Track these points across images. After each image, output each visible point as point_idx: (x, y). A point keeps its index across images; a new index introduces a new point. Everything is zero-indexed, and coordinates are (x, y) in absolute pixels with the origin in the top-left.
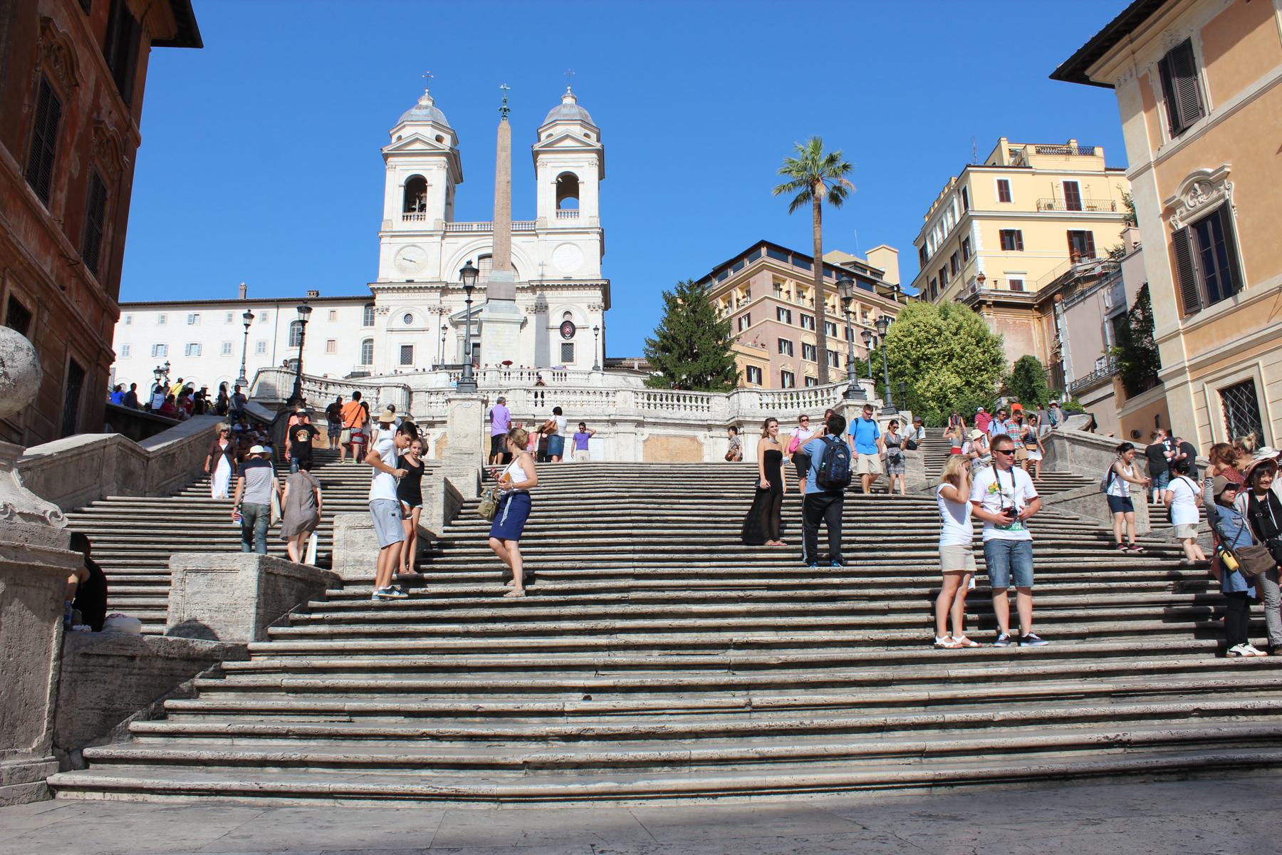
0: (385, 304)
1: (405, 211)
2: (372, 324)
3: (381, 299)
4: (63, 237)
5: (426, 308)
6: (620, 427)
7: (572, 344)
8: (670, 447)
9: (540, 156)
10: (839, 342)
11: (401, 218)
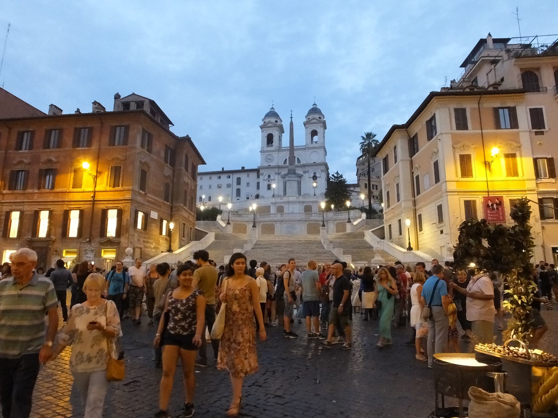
0: (263, 172)
1: (267, 144)
2: (259, 178)
3: (261, 172)
9: (306, 125)
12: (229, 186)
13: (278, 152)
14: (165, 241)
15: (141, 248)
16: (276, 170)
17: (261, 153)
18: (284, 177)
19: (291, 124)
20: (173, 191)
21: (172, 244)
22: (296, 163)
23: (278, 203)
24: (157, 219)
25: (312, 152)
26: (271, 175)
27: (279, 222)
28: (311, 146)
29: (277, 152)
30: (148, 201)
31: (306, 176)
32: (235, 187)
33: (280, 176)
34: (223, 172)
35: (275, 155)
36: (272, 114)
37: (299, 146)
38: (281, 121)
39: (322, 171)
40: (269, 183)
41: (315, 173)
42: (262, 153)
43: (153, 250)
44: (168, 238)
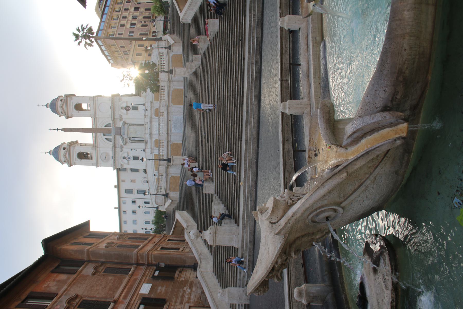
0: (120, 165)
1: (89, 159)
2: (126, 169)
4: (145, 243)
6: (170, 111)
9: (69, 116)
10: (129, 14)
12: (134, 202)
13: (97, 147)
14: (183, 273)
15: (190, 307)
16: (118, 150)
17: (98, 167)
18: (126, 143)
19: (65, 130)
20: (116, 263)
21: (187, 264)
22: (111, 127)
23: (151, 146)
24: (150, 285)
25: (100, 110)
26: (123, 156)
28: (92, 112)
29: (98, 149)
30: (125, 298)
31: (124, 117)
32: (135, 195)
33: (124, 146)
34: (119, 208)
35: (101, 151)
36: (56, 153)
37: (92, 124)
38: (65, 143)
39: (120, 100)
40: (132, 158)
41: (122, 108)
42: (99, 165)
43: (194, 289)
44: (179, 269)
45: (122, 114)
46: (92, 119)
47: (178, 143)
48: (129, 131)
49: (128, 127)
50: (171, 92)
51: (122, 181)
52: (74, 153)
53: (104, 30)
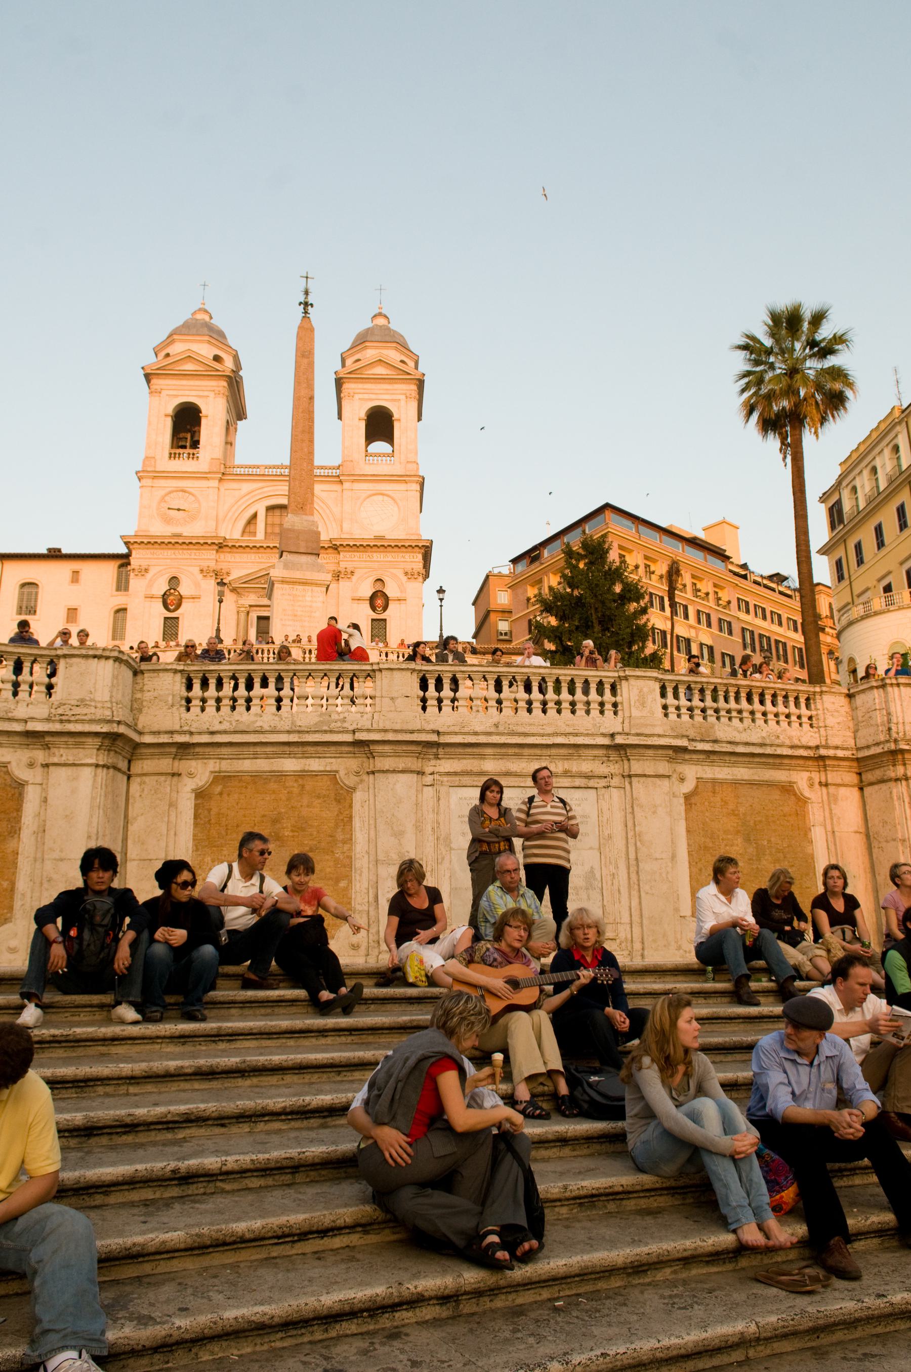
0: (144, 564)
1: (172, 447)
2: (126, 589)
5: (196, 570)
6: (637, 767)
7: (385, 620)
8: (742, 810)
10: (691, 627)
11: (167, 455)
13: (221, 480)
16: (209, 557)
19: (306, 332)
27: (411, 763)
29: (215, 483)
31: (344, 586)
42: (147, 482)
45: (354, 578)
46: (338, 468)
47: (349, 840)
48: (300, 587)
49: (317, 585)
50: (780, 776)
51: (76, 573)
52: (201, 393)
53: (640, 539)
